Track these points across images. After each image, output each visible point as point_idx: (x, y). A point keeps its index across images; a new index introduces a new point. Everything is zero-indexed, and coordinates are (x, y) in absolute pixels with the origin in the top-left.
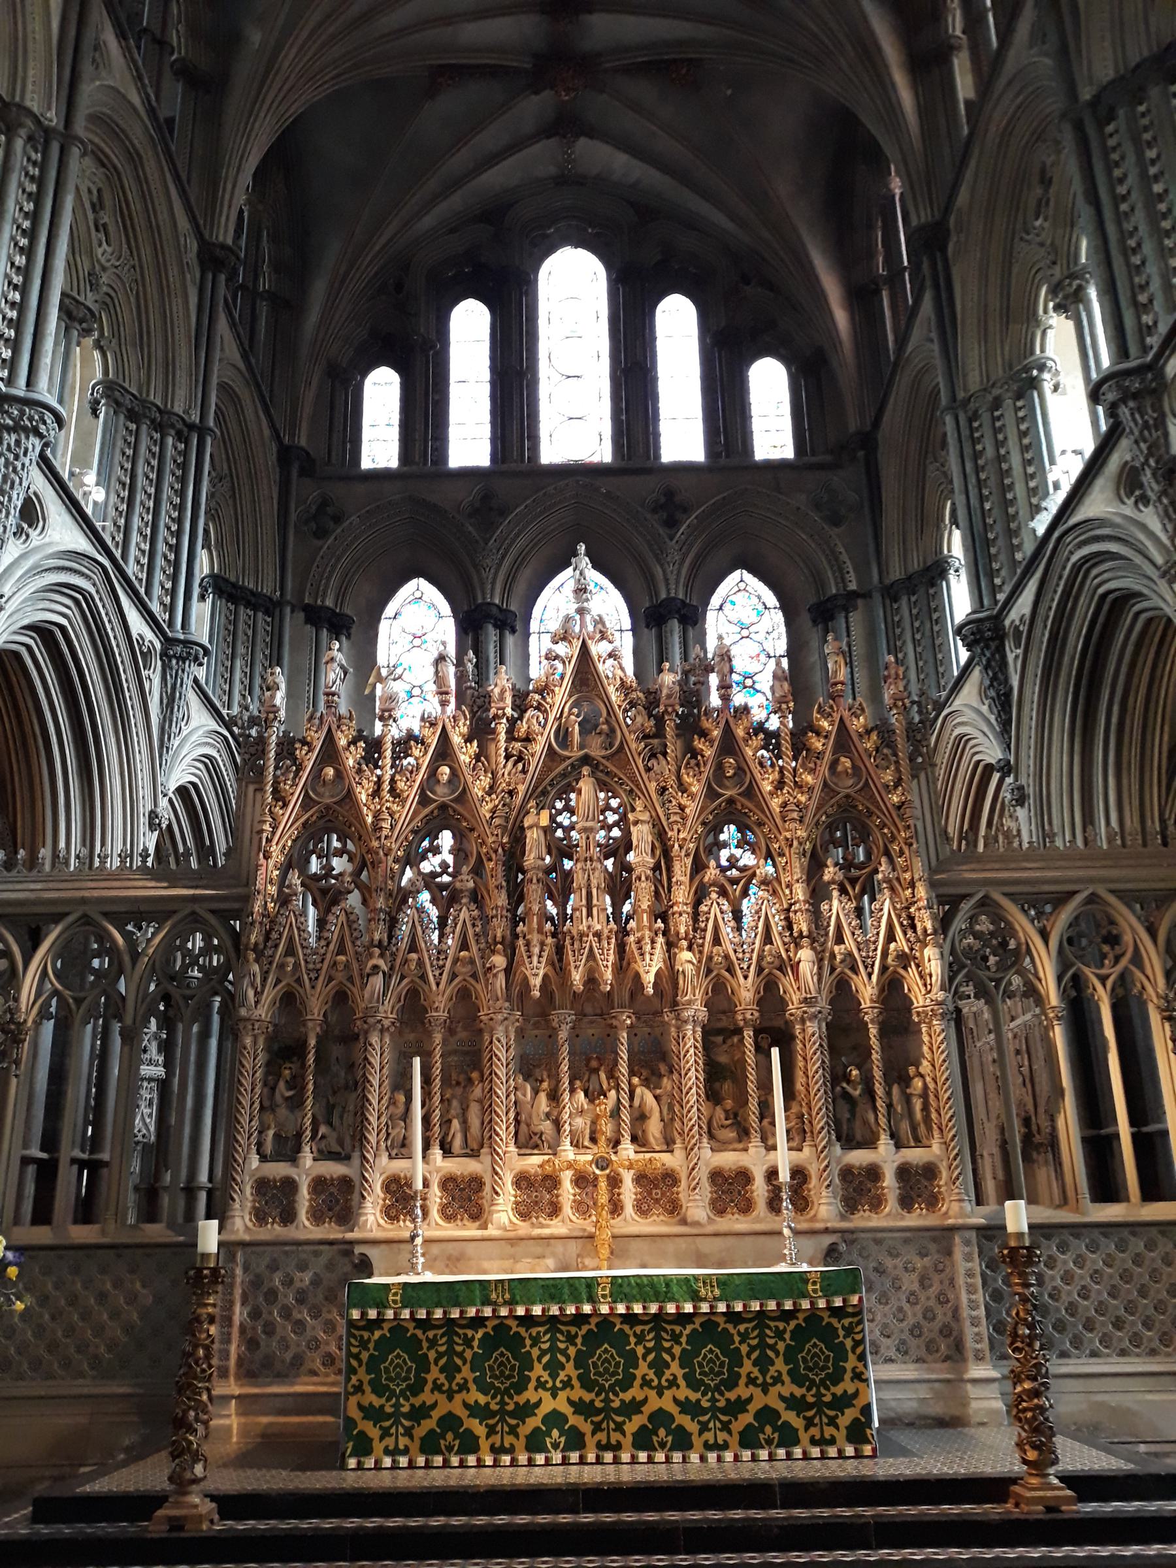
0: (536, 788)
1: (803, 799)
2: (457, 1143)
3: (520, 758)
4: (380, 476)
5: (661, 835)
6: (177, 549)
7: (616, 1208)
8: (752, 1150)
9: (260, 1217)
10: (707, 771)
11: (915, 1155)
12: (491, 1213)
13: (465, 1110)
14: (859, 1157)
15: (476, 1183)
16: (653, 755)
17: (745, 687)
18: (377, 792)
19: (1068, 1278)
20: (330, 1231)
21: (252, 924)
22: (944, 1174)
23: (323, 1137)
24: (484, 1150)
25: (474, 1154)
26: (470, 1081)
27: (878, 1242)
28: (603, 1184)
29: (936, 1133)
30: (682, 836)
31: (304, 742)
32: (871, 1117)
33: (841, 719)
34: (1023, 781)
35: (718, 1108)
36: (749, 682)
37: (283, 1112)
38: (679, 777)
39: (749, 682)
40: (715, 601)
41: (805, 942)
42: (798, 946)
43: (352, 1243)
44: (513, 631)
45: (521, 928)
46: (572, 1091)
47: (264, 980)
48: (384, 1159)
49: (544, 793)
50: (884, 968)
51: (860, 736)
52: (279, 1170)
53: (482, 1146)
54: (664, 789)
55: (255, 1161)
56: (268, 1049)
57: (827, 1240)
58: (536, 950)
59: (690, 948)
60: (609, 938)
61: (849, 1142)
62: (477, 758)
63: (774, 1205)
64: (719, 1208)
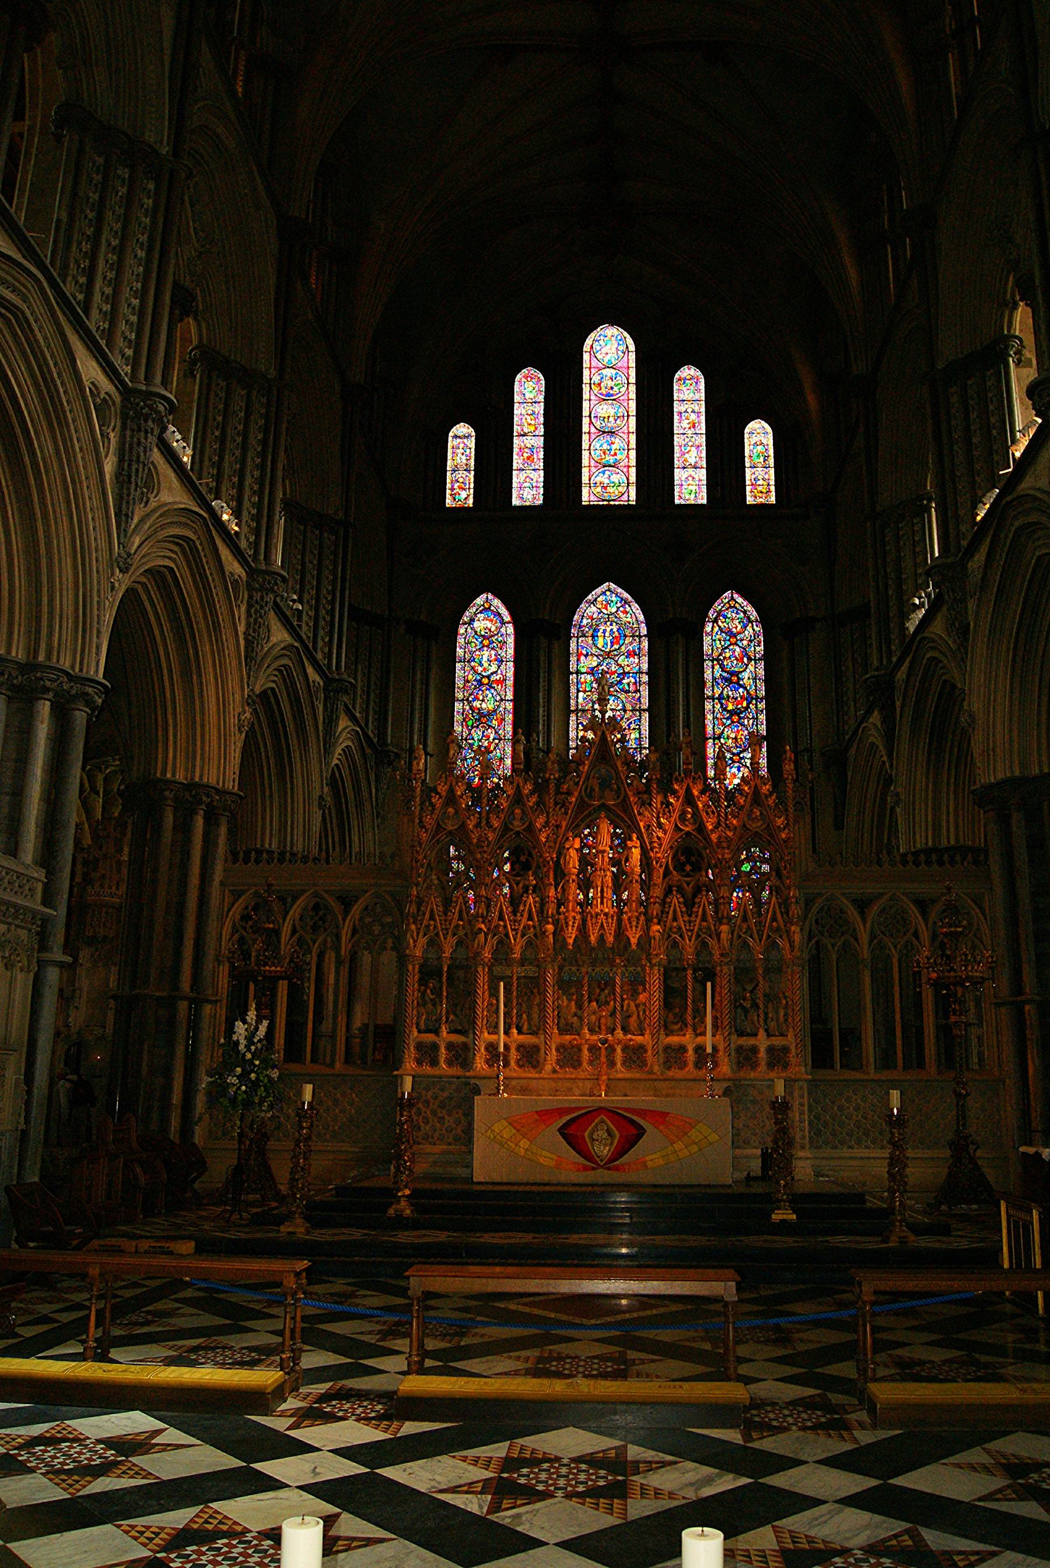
0: (572, 823)
1: (730, 834)
2: (525, 1027)
3: (563, 805)
4: (460, 511)
5: (644, 853)
6: (332, 613)
7: (612, 1064)
8: (688, 1036)
9: (419, 1062)
10: (676, 815)
11: (778, 1041)
12: (544, 1065)
13: (530, 1007)
14: (746, 1042)
15: (536, 1048)
16: (643, 804)
17: (731, 682)
18: (478, 825)
19: (857, 1108)
20: (455, 1071)
21: (411, 902)
22: (793, 1050)
23: (452, 1021)
24: (541, 1032)
25: (534, 1033)
26: (532, 993)
27: (754, 1086)
28: (603, 1051)
29: (791, 1030)
30: (659, 855)
31: (437, 793)
32: (756, 1018)
33: (756, 786)
34: (899, 790)
35: (670, 1015)
36: (735, 679)
37: (430, 1006)
38: (658, 818)
39: (735, 679)
40: (712, 614)
41: (725, 920)
42: (721, 923)
43: (469, 1078)
44: (558, 639)
45: (562, 909)
46: (590, 1002)
47: (418, 934)
48: (486, 1034)
49: (578, 825)
50: (769, 936)
51: (766, 796)
52: (430, 1037)
53: (539, 1029)
54: (649, 826)
55: (416, 1034)
56: (420, 972)
57: (726, 1085)
58: (571, 923)
59: (659, 924)
60: (612, 916)
61: (741, 1034)
62: (538, 804)
63: (700, 1063)
64: (667, 1065)
